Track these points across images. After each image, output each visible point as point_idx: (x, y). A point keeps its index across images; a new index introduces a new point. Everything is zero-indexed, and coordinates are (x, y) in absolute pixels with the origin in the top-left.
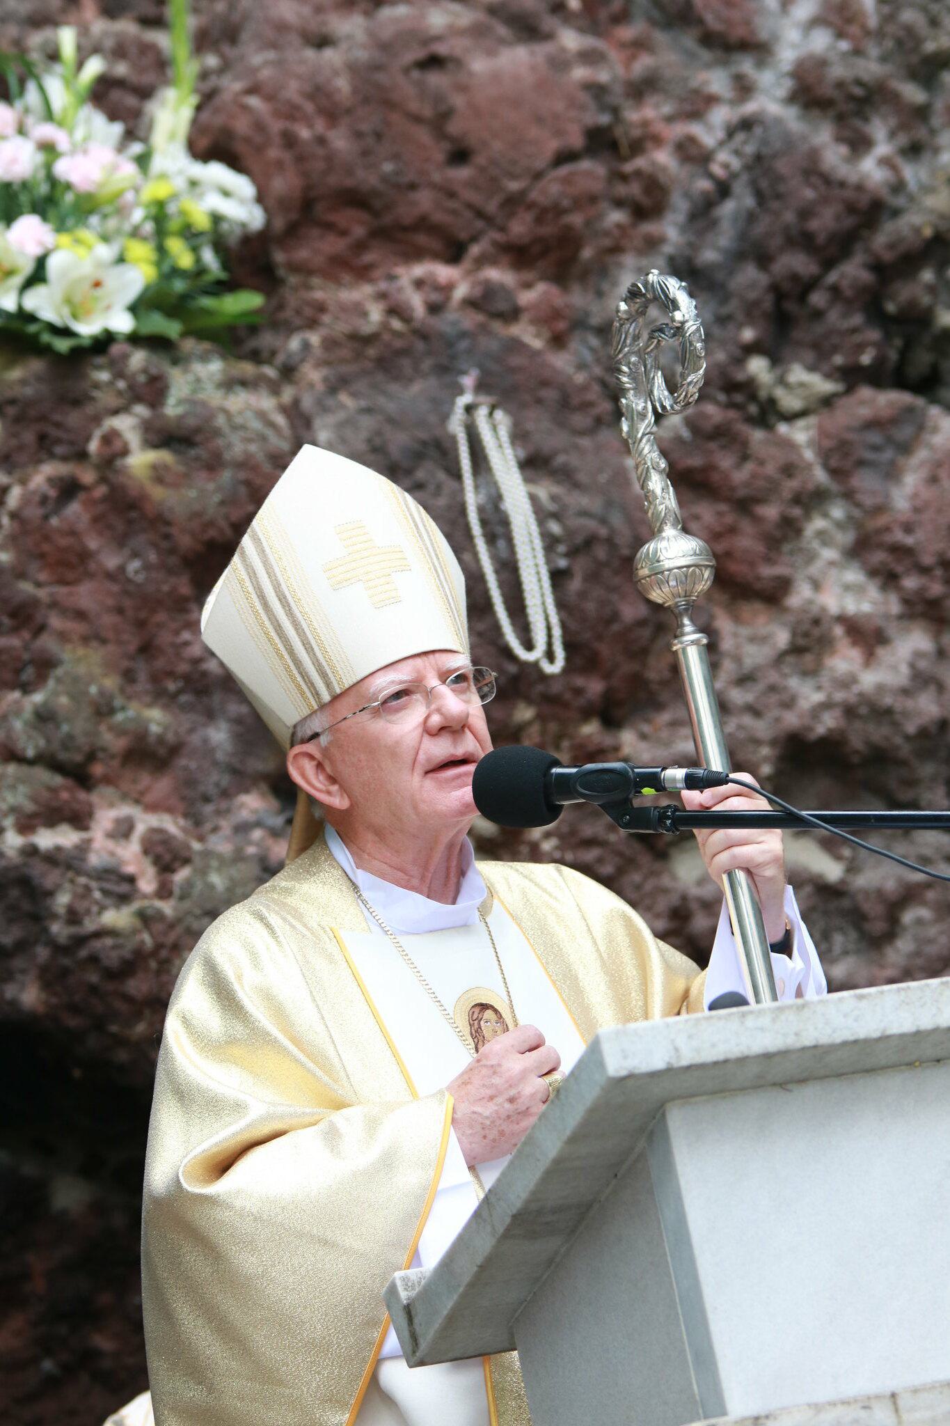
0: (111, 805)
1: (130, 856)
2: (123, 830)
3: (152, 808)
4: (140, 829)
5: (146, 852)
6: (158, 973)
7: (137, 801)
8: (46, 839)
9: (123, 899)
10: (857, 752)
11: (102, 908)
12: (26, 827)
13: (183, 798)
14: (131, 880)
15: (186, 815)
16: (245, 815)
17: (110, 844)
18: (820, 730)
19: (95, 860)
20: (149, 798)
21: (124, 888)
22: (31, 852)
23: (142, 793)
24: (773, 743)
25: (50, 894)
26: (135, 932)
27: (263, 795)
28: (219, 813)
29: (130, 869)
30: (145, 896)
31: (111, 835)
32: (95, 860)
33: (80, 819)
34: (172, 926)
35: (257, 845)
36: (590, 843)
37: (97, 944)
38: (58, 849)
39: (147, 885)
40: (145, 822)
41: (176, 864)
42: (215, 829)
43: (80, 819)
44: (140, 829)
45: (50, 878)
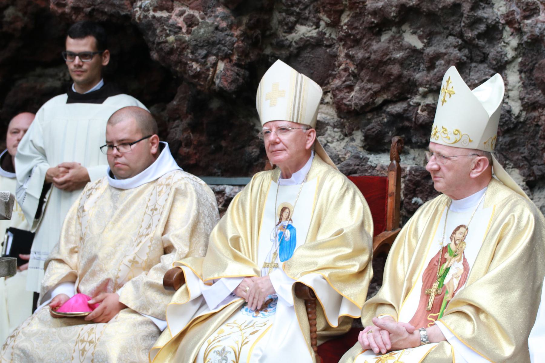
0: (179, 7)
1: (180, 22)
2: (181, 14)
3: (192, 8)
4: (187, 13)
5: (184, 21)
6: (180, 55)
7: (188, 6)
8: (158, 14)
9: (176, 33)
10: (424, 11)
11: (168, 35)
12: (155, 10)
13: (203, 6)
14: (180, 28)
15: (203, 11)
16: (217, 13)
17: (176, 17)
18: (411, 4)
19: (171, 21)
20: (191, 6)
21: (176, 30)
22: (154, 17)
23: (190, 4)
24: (396, 6)
25: (156, 29)
26: (172, 43)
27: (224, 8)
28: (212, 12)
29: (180, 25)
30: (183, 33)
31: (176, 15)
32: (171, 21)
33: (170, 9)
34: (184, 43)
35: (218, 22)
36: (356, 28)
37: (163, 45)
38: (161, 17)
39: (184, 30)
40: (189, 12)
41: (193, 25)
42: (211, 16)
43: (170, 9)
44: (187, 13)
45: (156, 25)
